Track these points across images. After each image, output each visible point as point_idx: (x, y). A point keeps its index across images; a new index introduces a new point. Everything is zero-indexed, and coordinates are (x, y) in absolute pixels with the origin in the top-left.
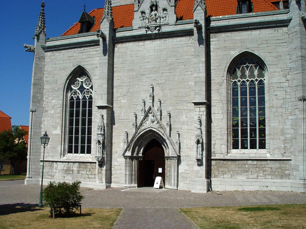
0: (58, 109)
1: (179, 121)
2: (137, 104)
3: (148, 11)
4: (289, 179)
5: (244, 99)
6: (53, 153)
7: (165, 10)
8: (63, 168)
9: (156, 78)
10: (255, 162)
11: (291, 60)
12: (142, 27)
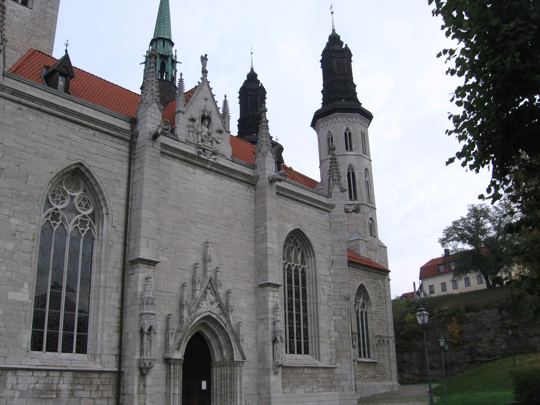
0: (25, 242)
1: (238, 307)
2: (185, 268)
4: (336, 391)
5: (289, 288)
6: (6, 347)
8: (32, 386)
9: (209, 233)
10: (310, 371)
11: (333, 253)
12: (192, 143)
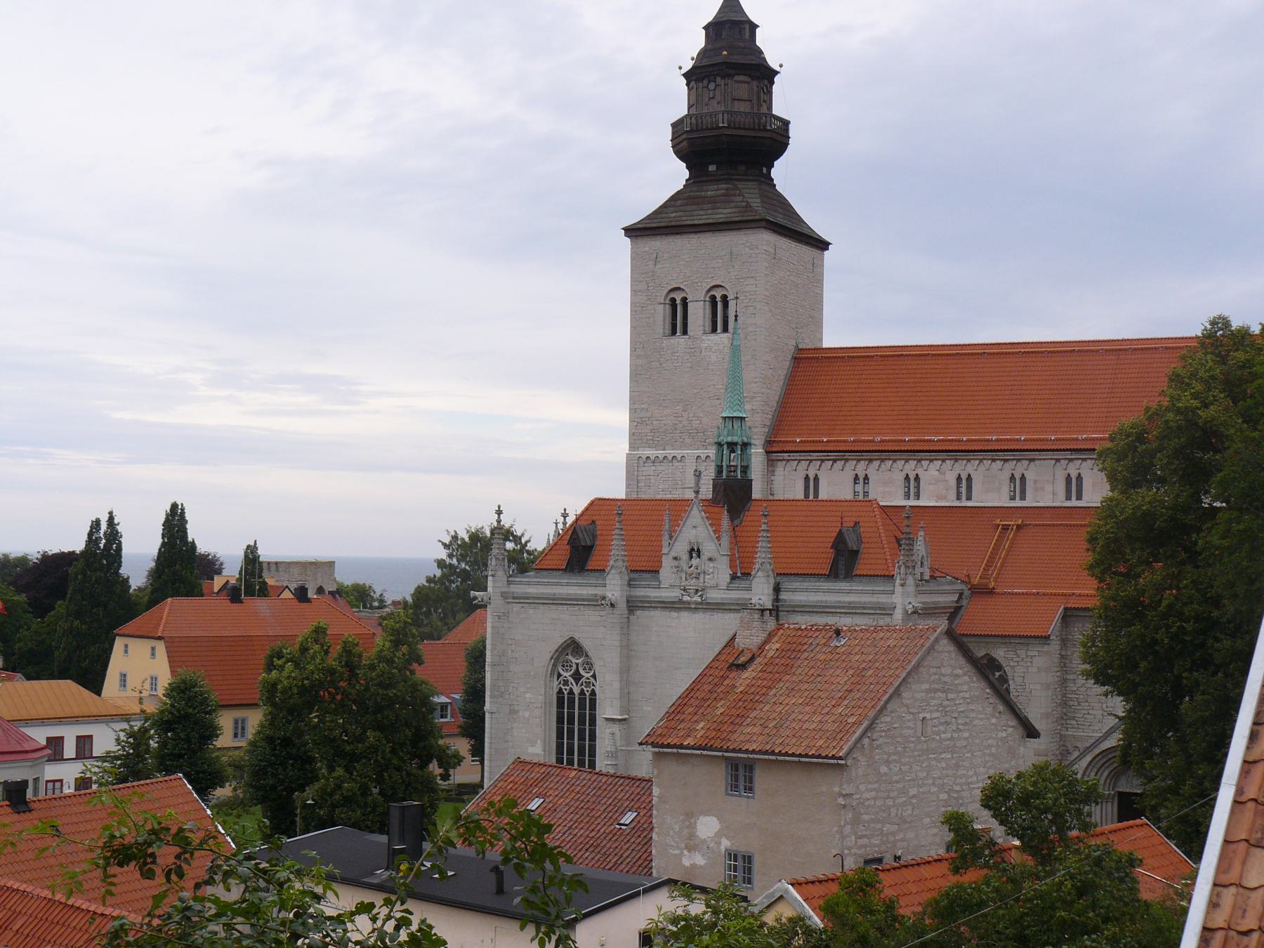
3: (685, 557)
7: (710, 559)
